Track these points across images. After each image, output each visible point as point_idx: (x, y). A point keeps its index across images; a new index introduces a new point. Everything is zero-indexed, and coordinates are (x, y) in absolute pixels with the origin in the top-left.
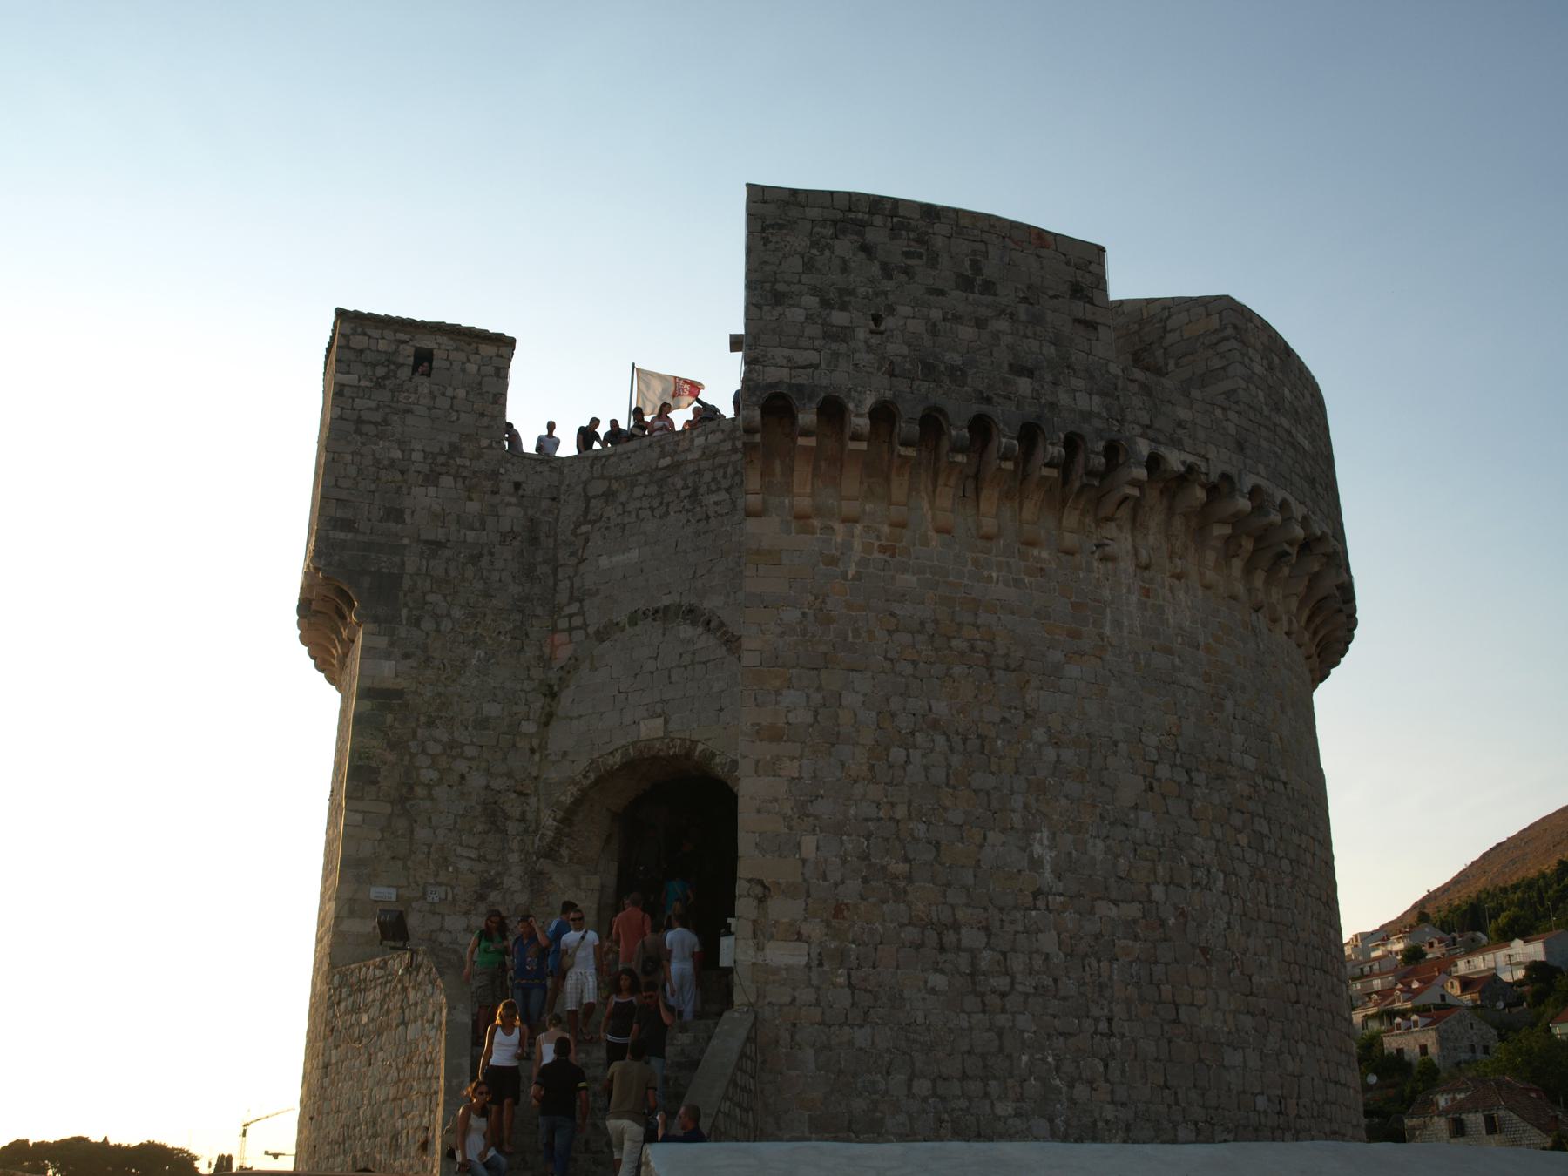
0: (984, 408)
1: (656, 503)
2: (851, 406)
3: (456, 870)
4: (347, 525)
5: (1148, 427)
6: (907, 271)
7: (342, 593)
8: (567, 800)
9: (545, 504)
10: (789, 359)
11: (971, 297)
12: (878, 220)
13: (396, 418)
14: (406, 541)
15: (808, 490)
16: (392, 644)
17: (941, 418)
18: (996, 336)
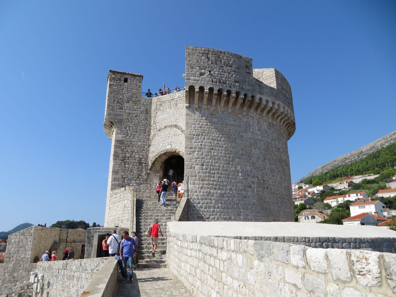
1: (169, 106)
3: (133, 172)
4: (113, 110)
5: (259, 92)
7: (112, 123)
8: (154, 160)
15: (197, 103)
16: (121, 132)
17: (222, 90)
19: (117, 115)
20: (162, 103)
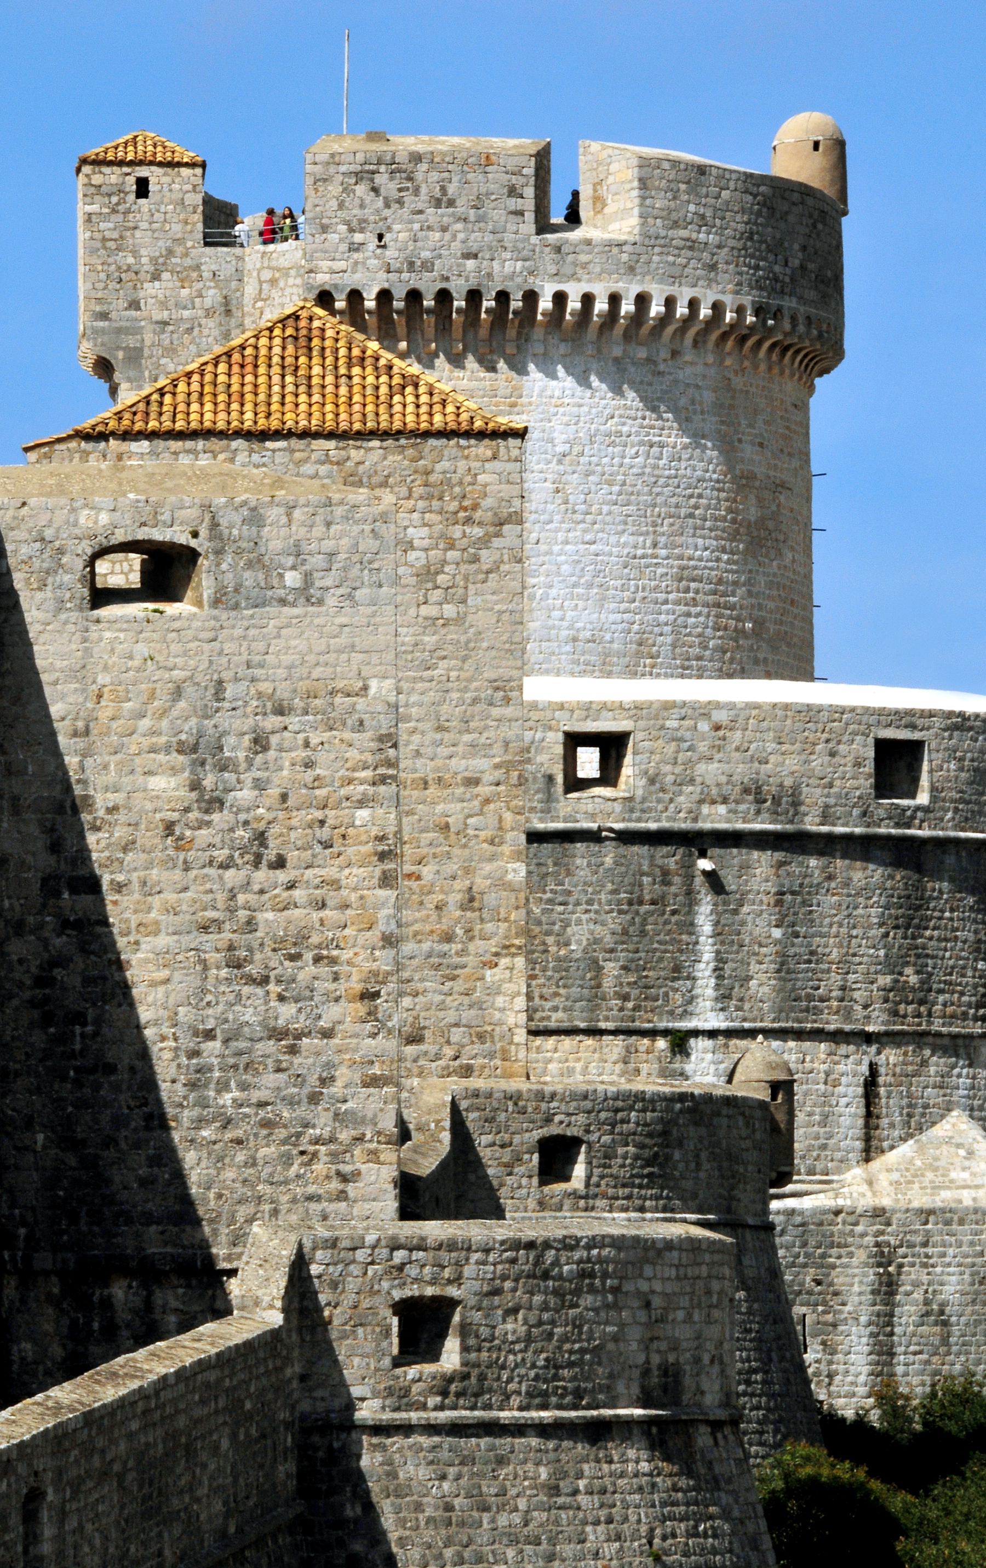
0: (444, 285)
2: (365, 295)
4: (104, 316)
6: (400, 202)
9: (234, 284)
10: (330, 268)
11: (439, 211)
12: (383, 168)
13: (128, 234)
14: (143, 323)
18: (454, 237)
19: (119, 331)
20: (277, 275)
